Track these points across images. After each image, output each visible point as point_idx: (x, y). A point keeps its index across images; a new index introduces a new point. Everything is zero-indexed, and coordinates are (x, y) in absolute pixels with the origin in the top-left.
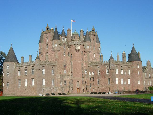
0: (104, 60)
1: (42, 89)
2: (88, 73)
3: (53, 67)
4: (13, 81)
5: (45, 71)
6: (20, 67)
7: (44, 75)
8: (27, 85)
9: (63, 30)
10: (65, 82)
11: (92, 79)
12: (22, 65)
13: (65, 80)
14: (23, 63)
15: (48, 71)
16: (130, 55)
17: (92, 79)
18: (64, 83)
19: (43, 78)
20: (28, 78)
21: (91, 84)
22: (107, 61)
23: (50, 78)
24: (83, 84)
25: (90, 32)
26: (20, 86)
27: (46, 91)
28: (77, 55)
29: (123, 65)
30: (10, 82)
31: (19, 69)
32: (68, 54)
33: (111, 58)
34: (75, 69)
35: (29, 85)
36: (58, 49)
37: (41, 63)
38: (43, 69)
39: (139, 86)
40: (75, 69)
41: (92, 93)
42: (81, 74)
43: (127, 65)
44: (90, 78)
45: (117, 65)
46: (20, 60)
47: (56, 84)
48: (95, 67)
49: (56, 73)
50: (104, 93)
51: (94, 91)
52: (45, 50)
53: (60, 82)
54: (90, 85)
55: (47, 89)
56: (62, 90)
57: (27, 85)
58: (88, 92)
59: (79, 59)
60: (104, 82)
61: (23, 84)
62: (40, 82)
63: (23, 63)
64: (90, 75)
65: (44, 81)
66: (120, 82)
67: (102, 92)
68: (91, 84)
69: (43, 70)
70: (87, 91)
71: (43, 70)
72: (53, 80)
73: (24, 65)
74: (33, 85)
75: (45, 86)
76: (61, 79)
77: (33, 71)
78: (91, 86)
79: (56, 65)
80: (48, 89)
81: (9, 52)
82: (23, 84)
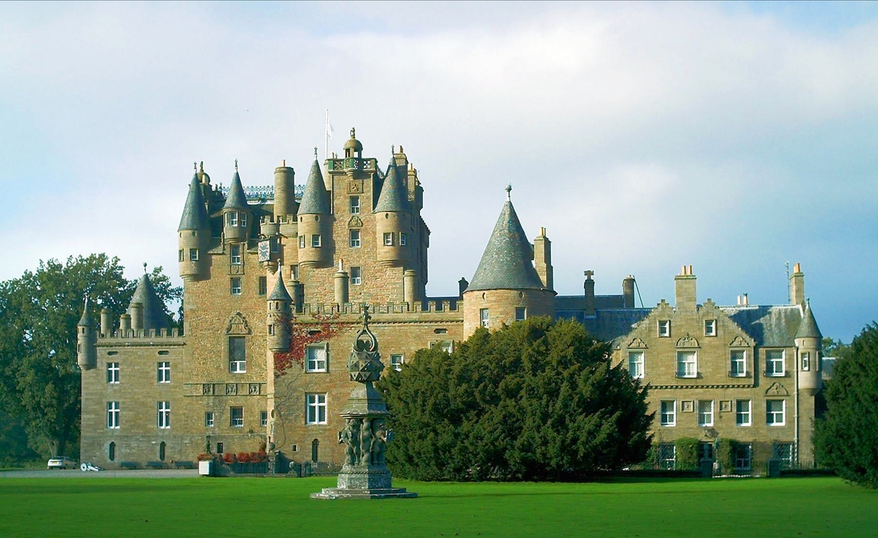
1: (101, 446)
3: (160, 353)
5: (122, 370)
7: (116, 388)
10: (236, 412)
13: (232, 403)
18: (228, 415)
19: (111, 400)
23: (149, 400)
27: (123, 451)
38: (110, 365)
43: (415, 317)
49: (180, 375)
53: (203, 414)
55: (128, 446)
62: (93, 416)
79: (181, 340)
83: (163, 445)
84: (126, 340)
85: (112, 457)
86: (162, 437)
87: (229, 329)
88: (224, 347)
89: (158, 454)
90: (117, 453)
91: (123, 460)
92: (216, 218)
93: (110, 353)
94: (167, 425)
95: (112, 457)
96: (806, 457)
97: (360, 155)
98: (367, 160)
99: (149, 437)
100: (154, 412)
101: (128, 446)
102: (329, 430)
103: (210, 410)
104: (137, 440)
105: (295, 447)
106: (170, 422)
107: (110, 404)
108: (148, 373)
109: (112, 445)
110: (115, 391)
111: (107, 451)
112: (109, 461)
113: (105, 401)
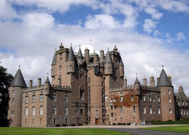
0: (128, 84)
1: (52, 119)
2: (109, 100)
3: (66, 93)
4: (19, 109)
6: (28, 93)
8: (34, 114)
9: (80, 50)
11: (114, 107)
12: (30, 90)
13: (81, 108)
14: (31, 87)
16: (158, 79)
17: (114, 107)
18: (80, 111)
19: (54, 106)
20: (36, 106)
21: (112, 113)
22: (131, 86)
24: (103, 113)
25: (112, 52)
26: (27, 114)
27: (57, 121)
28: (96, 79)
30: (16, 110)
31: (27, 95)
32: (85, 77)
33: (137, 82)
34: (94, 96)
35: (37, 114)
39: (171, 116)
40: (94, 96)
41: (114, 124)
42: (100, 101)
44: (112, 106)
46: (28, 84)
47: (70, 113)
48: (118, 93)
50: (129, 124)
51: (116, 122)
52: (59, 73)
53: (75, 110)
54: (111, 114)
56: (78, 121)
57: (34, 114)
58: (109, 123)
59: (98, 84)
60: (128, 111)
61: (30, 113)
63: (31, 87)
64: (111, 102)
65: (55, 110)
66: (148, 112)
67: (126, 123)
68: (112, 113)
70: (108, 122)
72: (67, 109)
73: (32, 89)
74: (42, 114)
77: (42, 96)
78: (112, 116)
81: (16, 75)
82: (30, 113)
83: (67, 119)
85: (54, 123)
88: (79, 93)
89: (65, 122)
95: (54, 123)
96: (174, 120)
100: (64, 110)
101: (58, 119)
107: (53, 107)
109: (55, 119)
110: (55, 103)
111: (53, 121)
113: (53, 106)
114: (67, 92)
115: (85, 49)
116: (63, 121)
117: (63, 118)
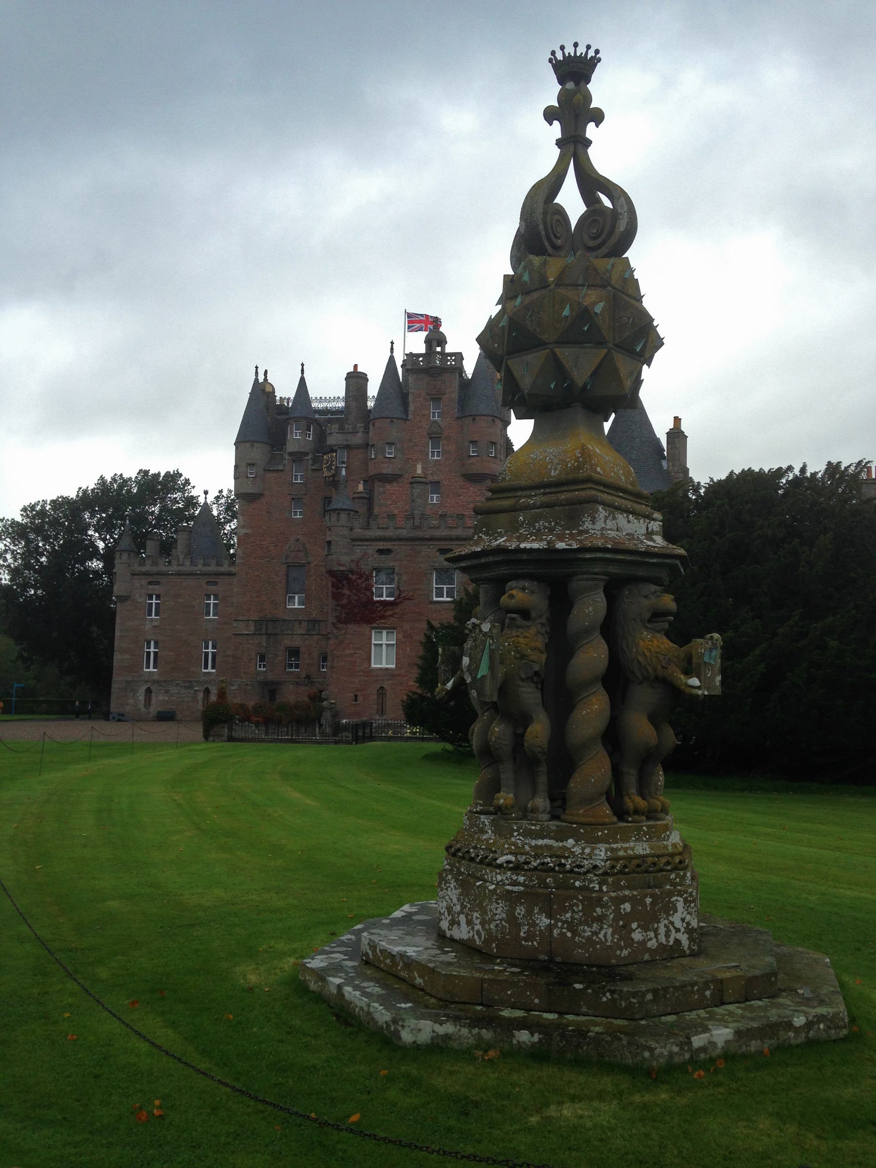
7: (155, 624)
15: (181, 600)
19: (149, 638)
27: (161, 698)
29: (458, 539)
36: (244, 491)
37: (137, 568)
38: (151, 598)
45: (382, 545)
62: (127, 656)
69: (154, 601)
71: (154, 601)
75: (156, 677)
76: (264, 640)
79: (233, 570)
80: (174, 690)
84: (170, 568)
86: (206, 682)
87: (287, 557)
90: (154, 701)
91: (160, 709)
92: (271, 425)
93: (150, 583)
94: (213, 668)
97: (443, 349)
98: (451, 355)
99: (190, 682)
101: (167, 692)
102: (399, 675)
103: (263, 651)
104: (177, 685)
105: (356, 696)
106: (217, 665)
107: (149, 643)
108: (193, 606)
109: (149, 691)
110: (155, 627)
112: (143, 709)
114: (213, 578)
115: (352, 370)
116: (186, 699)
117: (186, 687)
